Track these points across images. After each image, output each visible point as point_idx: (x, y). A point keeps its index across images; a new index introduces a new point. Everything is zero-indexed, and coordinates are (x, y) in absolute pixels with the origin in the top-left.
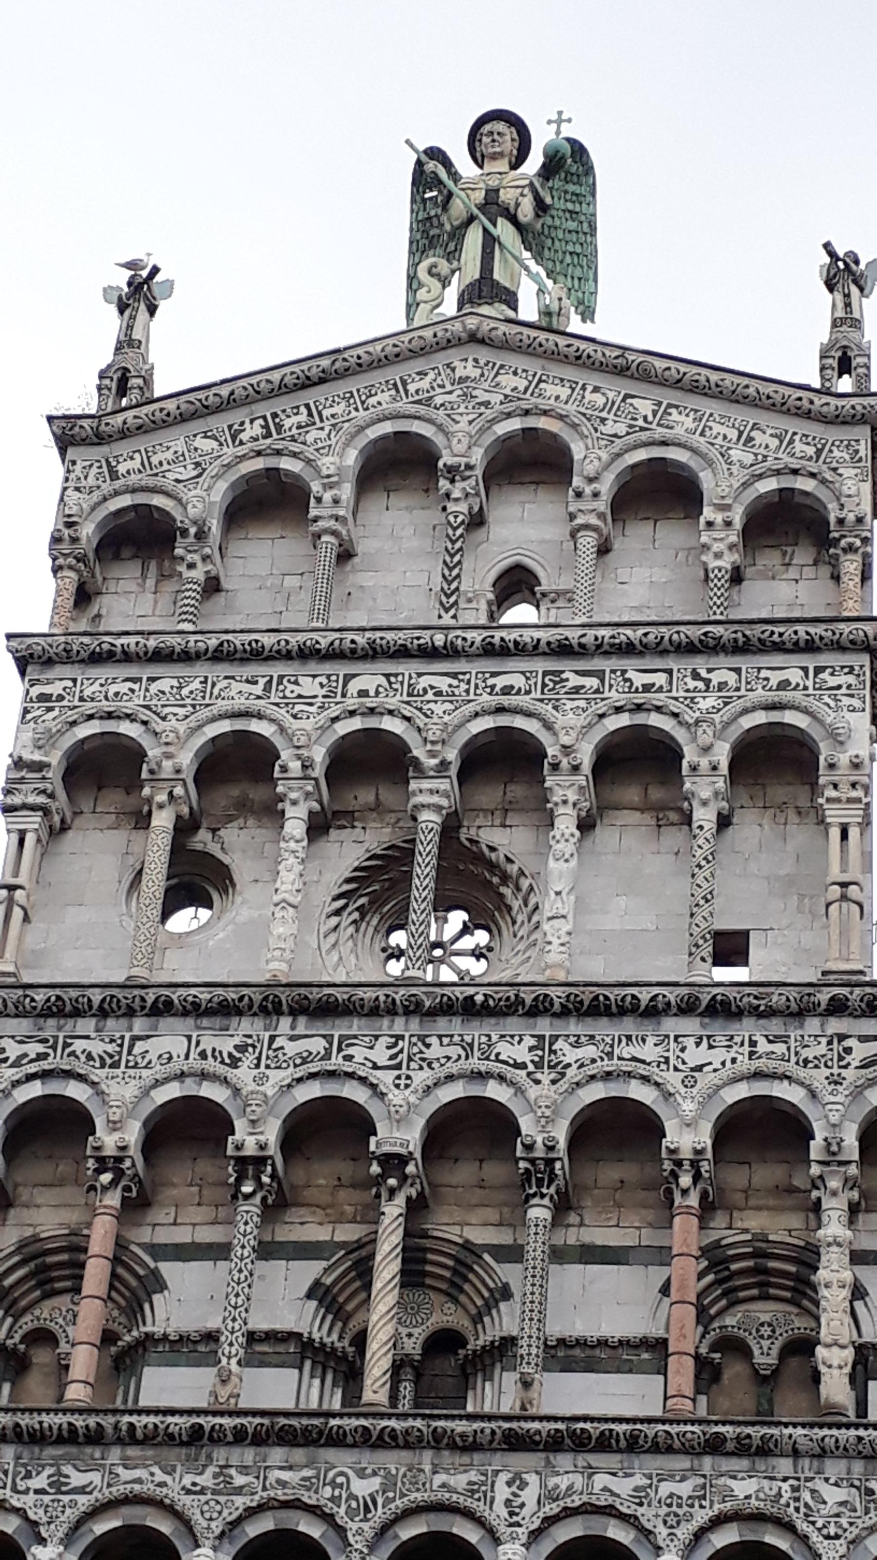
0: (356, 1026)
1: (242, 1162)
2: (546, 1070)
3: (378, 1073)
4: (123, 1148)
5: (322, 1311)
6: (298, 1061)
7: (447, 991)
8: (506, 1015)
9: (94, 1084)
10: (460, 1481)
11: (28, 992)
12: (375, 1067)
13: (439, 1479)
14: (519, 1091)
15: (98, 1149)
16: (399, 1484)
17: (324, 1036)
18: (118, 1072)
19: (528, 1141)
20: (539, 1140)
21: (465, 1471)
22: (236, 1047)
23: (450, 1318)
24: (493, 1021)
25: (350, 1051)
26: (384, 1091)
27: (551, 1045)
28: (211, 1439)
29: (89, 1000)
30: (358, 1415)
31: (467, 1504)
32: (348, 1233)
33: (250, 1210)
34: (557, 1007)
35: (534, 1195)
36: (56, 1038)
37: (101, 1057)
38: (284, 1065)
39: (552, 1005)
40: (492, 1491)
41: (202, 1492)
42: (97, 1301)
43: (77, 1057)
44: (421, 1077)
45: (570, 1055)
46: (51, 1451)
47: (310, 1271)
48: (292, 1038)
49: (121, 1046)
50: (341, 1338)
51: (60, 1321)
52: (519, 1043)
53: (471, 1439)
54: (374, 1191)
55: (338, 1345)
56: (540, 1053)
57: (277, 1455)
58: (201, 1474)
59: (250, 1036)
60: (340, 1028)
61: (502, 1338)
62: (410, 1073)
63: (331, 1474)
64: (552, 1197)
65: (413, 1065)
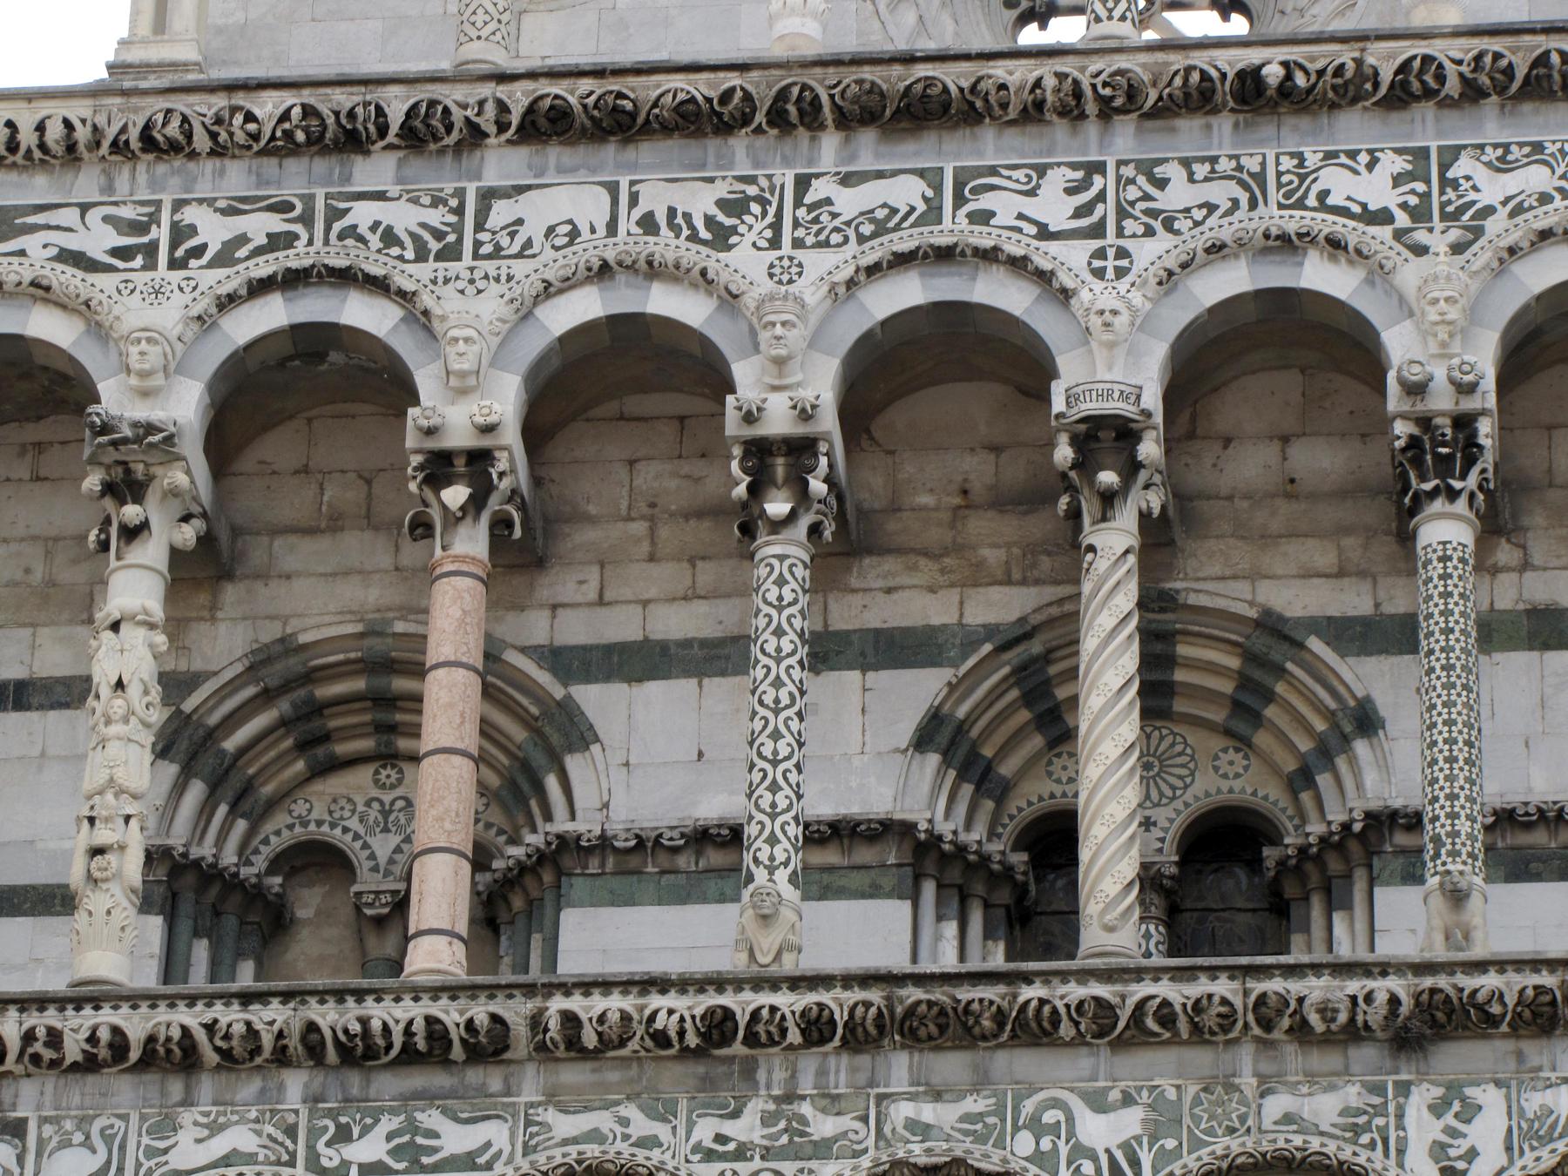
0: (989, 147)
1: (759, 451)
2: (1438, 224)
3: (1053, 247)
4: (488, 429)
5: (952, 774)
6: (867, 229)
7: (1200, 59)
8: (1334, 106)
9: (405, 297)
10: (1325, 1107)
11: (240, 99)
12: (1044, 233)
13: (1276, 1105)
14: (1379, 274)
15: (430, 432)
16: (1187, 1120)
17: (921, 173)
18: (454, 267)
19: (1415, 374)
20: (1440, 373)
21: (1332, 1088)
22: (722, 204)
23: (1237, 784)
24: (1304, 122)
25: (985, 202)
26: (1069, 283)
27: (1444, 168)
28: (751, 1039)
29: (379, 109)
30: (1084, 975)
31: (1346, 1155)
32: (1000, 606)
33: (784, 557)
34: (1452, 86)
35: (1433, 494)
36: (309, 200)
37: (415, 237)
38: (836, 238)
39: (1441, 78)
40: (1400, 1126)
41: (741, 1153)
42: (457, 760)
43: (361, 239)
44: (1151, 252)
45: (1492, 189)
46: (388, 1084)
47: (917, 691)
48: (847, 180)
49: (459, 211)
50: (992, 834)
51: (353, 823)
52: (1370, 166)
53: (1343, 1017)
54: (1064, 502)
55: (994, 848)
56: (1420, 187)
57: (899, 1066)
58: (736, 1115)
59: (751, 180)
60: (950, 154)
61: (1369, 815)
62: (1121, 242)
63: (1028, 1107)
64: (1472, 496)
65: (1130, 226)
